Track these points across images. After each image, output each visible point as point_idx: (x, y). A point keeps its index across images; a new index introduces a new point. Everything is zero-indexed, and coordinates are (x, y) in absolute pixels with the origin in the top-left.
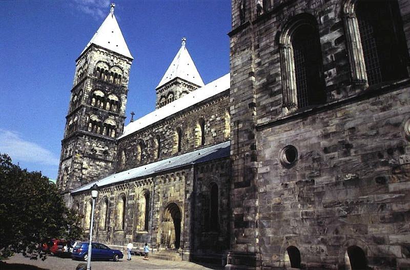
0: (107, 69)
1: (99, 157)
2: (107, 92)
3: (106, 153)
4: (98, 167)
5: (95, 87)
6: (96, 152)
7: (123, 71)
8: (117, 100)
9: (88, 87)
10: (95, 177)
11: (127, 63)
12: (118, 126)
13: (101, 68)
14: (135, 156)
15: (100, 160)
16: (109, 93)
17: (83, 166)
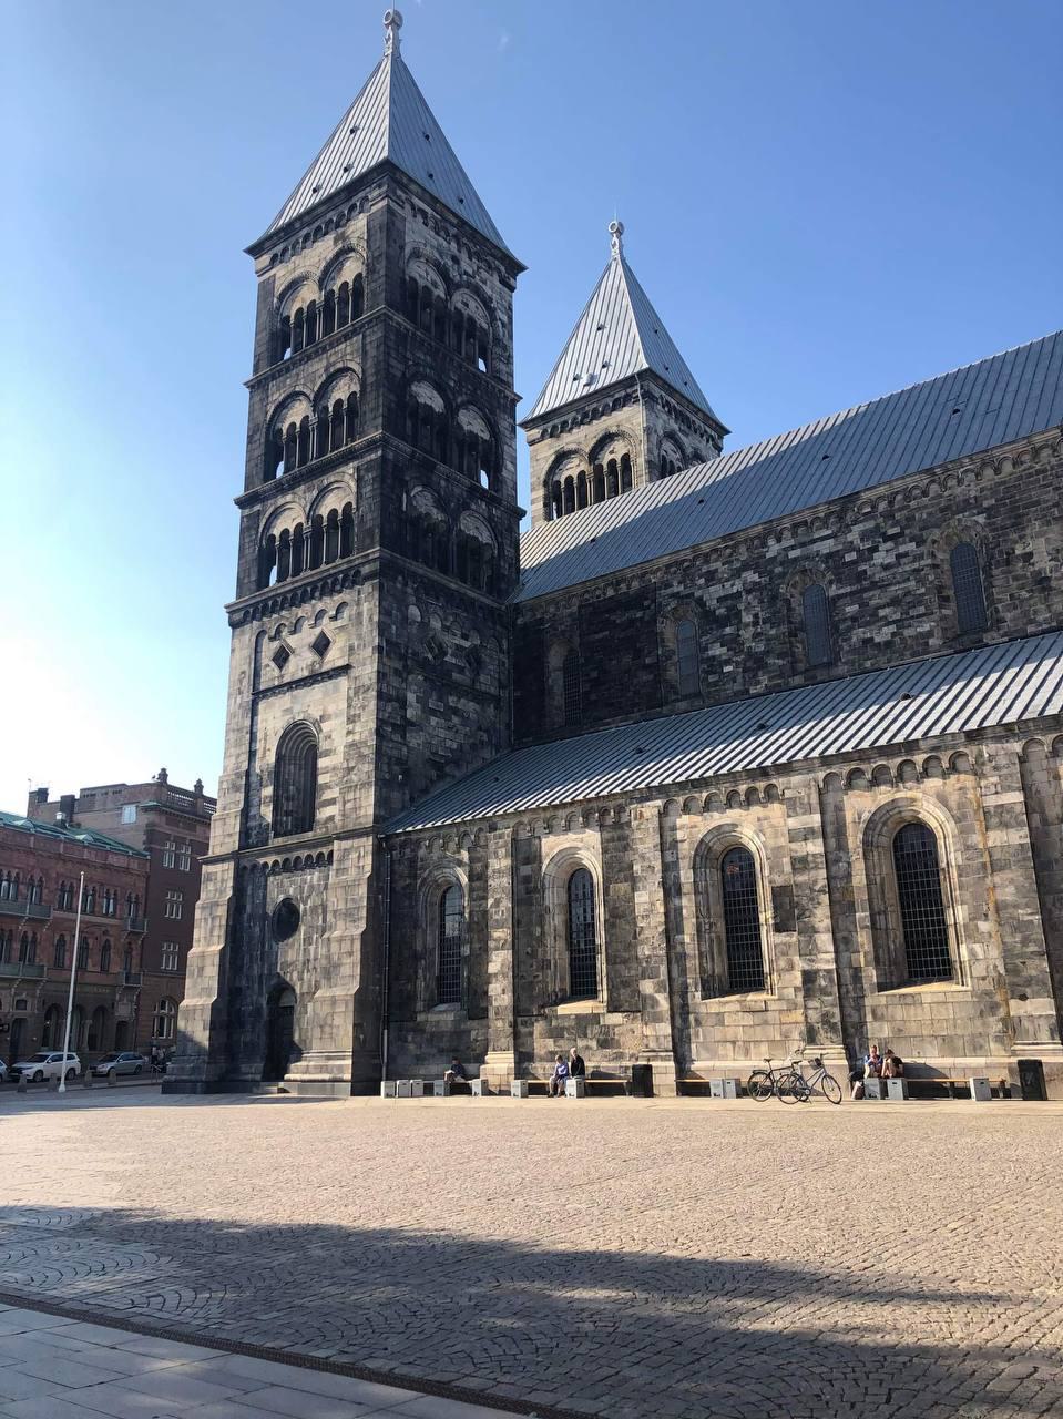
0: (440, 292)
1: (455, 676)
2: (452, 390)
3: (474, 659)
4: (455, 720)
5: (416, 364)
6: (445, 654)
7: (491, 311)
8: (486, 436)
9: (393, 362)
10: (449, 761)
11: (503, 282)
12: (501, 546)
13: (421, 282)
14: (646, 667)
15: (456, 689)
16: (459, 400)
17: (410, 713)
